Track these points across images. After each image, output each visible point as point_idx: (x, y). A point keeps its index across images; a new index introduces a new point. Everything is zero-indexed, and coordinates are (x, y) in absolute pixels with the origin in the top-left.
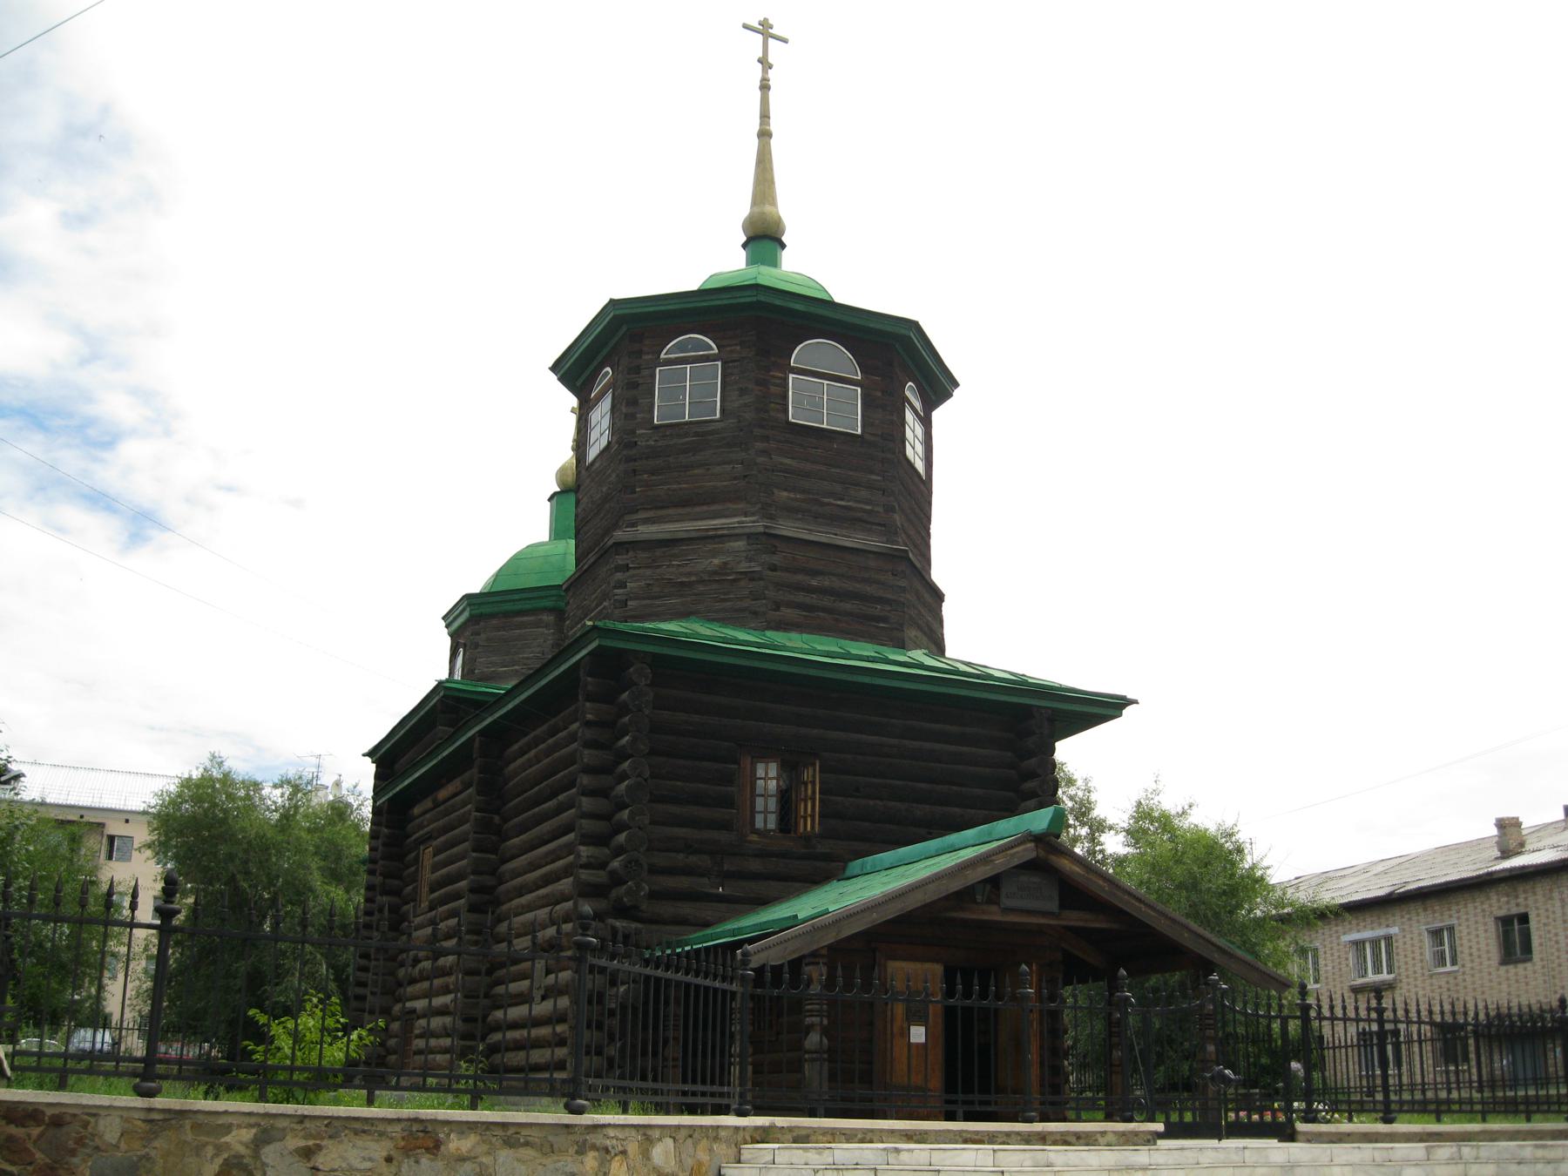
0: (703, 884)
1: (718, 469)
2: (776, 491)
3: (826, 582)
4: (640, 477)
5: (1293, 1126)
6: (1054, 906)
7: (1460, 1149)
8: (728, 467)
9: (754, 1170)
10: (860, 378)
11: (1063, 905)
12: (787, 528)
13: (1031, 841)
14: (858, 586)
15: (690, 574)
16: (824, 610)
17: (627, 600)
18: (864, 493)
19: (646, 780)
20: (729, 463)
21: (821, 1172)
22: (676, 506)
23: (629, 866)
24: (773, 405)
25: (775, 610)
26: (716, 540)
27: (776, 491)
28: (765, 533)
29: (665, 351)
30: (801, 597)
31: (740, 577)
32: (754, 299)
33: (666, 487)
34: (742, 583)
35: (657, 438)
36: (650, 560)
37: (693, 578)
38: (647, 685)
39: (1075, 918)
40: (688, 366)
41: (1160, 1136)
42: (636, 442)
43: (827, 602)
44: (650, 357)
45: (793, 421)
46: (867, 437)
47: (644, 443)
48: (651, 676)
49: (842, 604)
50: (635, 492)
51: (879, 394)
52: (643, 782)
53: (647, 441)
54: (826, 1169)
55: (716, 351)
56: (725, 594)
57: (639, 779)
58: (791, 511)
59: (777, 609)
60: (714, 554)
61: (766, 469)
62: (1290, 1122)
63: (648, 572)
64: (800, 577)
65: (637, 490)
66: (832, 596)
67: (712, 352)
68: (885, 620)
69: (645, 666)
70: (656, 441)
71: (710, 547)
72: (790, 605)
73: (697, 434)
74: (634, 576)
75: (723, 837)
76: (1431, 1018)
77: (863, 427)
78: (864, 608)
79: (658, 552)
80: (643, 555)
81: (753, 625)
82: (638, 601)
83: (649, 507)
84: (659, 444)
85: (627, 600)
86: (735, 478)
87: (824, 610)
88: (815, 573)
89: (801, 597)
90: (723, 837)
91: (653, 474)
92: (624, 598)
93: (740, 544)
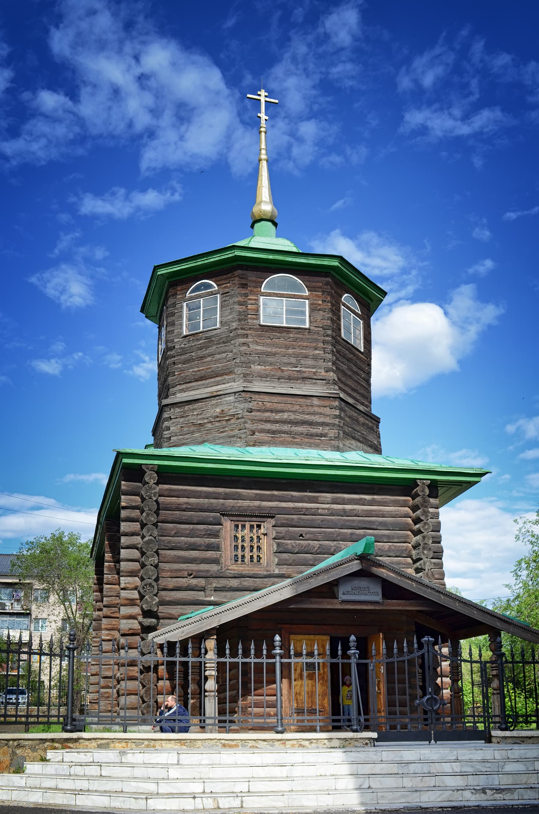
0: (200, 596)
1: (218, 356)
2: (252, 366)
3: (285, 416)
4: (177, 366)
5: (490, 733)
6: (378, 598)
7: (178, 761)
8: (224, 355)
9: (40, 765)
10: (307, 294)
11: (385, 596)
12: (258, 386)
13: (357, 559)
14: (306, 416)
15: (204, 419)
16: (285, 432)
17: (170, 437)
18: (310, 362)
19: (155, 538)
20: (224, 353)
21: (73, 767)
22: (196, 381)
23: (145, 587)
24: (249, 316)
25: (251, 435)
26: (217, 398)
27: (252, 366)
28: (244, 391)
29: (189, 292)
30: (268, 426)
31: (231, 418)
32: (233, 255)
33: (191, 371)
34: (232, 421)
35: (185, 343)
36: (182, 413)
37: (206, 421)
38: (154, 483)
39: (395, 605)
40: (202, 299)
41: (377, 740)
42: (174, 346)
43: (286, 427)
44: (181, 296)
45: (263, 324)
46: (312, 328)
47: (178, 347)
48: (157, 478)
49: (296, 428)
50: (175, 375)
51: (320, 302)
52: (154, 539)
53: (180, 345)
54: (76, 765)
55: (217, 288)
56: (223, 428)
57: (151, 537)
58: (263, 377)
59: (253, 433)
60: (216, 405)
61: (246, 354)
62: (488, 730)
63: (182, 420)
64: (268, 414)
65: (176, 374)
66: (289, 424)
67: (214, 289)
68: (325, 435)
69: (153, 472)
70: (185, 344)
71: (214, 402)
72: (262, 431)
73: (206, 338)
74: (174, 423)
75: (214, 568)
76: (523, 660)
77: (310, 322)
78: (312, 430)
79: (186, 408)
80: (178, 410)
81: (239, 445)
82: (176, 437)
83: (182, 383)
84: (187, 346)
85: (170, 437)
86: (228, 361)
87: (285, 432)
88: (278, 411)
89: (268, 426)
90: (214, 568)
91: (184, 364)
92: (170, 436)
93: (231, 398)
